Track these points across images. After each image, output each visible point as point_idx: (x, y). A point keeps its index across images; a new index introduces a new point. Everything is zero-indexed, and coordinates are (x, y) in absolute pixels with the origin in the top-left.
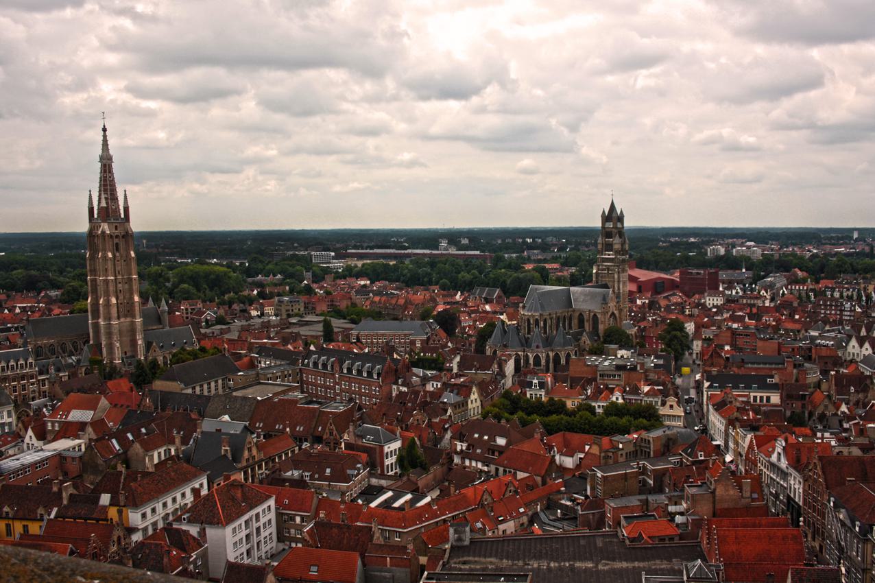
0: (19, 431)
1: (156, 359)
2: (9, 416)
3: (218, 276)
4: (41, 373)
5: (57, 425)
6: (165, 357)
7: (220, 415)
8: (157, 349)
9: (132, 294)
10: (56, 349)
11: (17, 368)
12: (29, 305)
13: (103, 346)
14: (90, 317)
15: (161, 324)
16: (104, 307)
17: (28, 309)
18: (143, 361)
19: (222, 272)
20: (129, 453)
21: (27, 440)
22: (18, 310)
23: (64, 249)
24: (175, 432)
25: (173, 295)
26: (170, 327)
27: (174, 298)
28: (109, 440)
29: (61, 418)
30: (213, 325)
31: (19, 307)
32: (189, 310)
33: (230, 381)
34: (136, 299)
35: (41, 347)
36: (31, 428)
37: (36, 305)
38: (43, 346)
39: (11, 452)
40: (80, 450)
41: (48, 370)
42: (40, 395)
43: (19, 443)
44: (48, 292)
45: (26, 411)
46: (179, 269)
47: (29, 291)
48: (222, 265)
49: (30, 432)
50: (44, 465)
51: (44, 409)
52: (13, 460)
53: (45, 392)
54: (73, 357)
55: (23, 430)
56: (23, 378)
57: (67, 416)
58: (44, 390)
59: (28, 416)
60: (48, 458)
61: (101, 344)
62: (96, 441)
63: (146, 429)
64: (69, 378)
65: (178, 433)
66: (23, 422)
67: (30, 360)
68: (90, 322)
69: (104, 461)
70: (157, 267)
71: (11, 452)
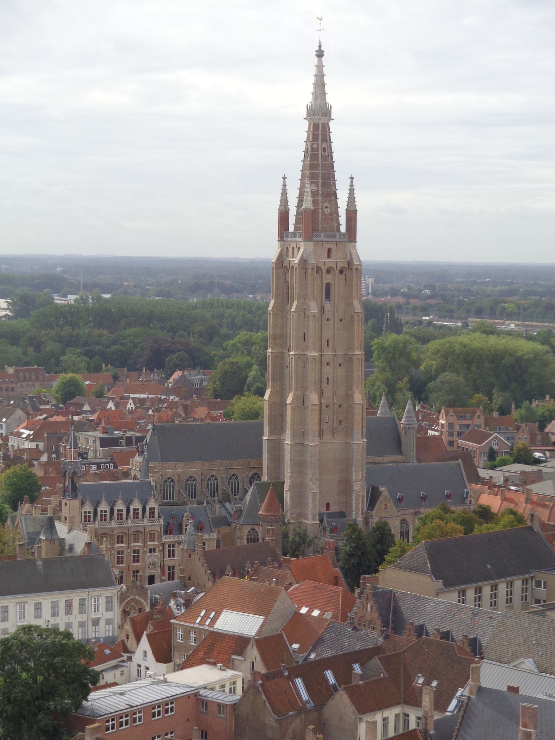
0: (123, 637)
1: (386, 524)
2: (109, 608)
3: (519, 360)
4: (168, 531)
5: (192, 635)
6: (403, 521)
7: (515, 656)
8: (391, 505)
9: (349, 388)
10: (198, 486)
11: (127, 518)
12: (150, 396)
13: (286, 488)
14: (266, 429)
15: (401, 453)
16: (293, 409)
17: (148, 405)
18: (361, 526)
19: (528, 353)
20: (325, 710)
21: (137, 657)
22: (130, 406)
23: (216, 290)
24: (421, 681)
25: (423, 396)
26: (419, 461)
27: (426, 400)
28: (291, 678)
29: (202, 623)
30: (504, 463)
31: (133, 399)
32: (457, 428)
33: (538, 584)
34: (358, 398)
35: (172, 481)
36: (148, 636)
37: (163, 397)
38: (175, 479)
39: (109, 677)
40: (233, 691)
41: (181, 525)
42: (163, 574)
43: (123, 661)
44: (186, 373)
45: (137, 602)
46: (442, 341)
47: (152, 370)
48: (530, 338)
49: (145, 643)
50: (167, 711)
51: (172, 603)
52: (115, 693)
53: (173, 568)
54: (227, 505)
55: (132, 637)
56: (137, 535)
57: (214, 621)
58: (171, 564)
59: (140, 610)
60: (173, 700)
61: (283, 483)
62: (266, 677)
63: (362, 666)
64: (218, 547)
65: (427, 683)
66: (134, 623)
67: (152, 504)
68: (265, 437)
69: (277, 720)
70: (395, 336)
71: (109, 677)
